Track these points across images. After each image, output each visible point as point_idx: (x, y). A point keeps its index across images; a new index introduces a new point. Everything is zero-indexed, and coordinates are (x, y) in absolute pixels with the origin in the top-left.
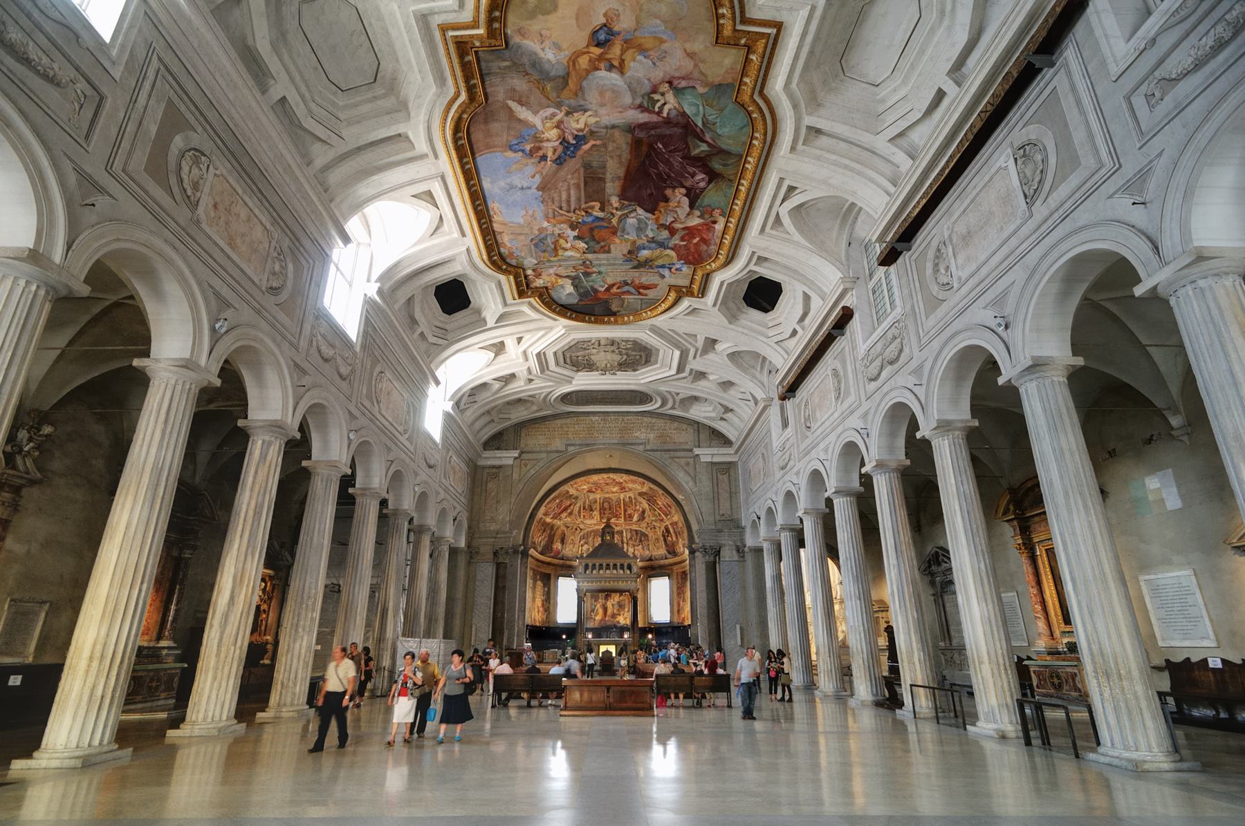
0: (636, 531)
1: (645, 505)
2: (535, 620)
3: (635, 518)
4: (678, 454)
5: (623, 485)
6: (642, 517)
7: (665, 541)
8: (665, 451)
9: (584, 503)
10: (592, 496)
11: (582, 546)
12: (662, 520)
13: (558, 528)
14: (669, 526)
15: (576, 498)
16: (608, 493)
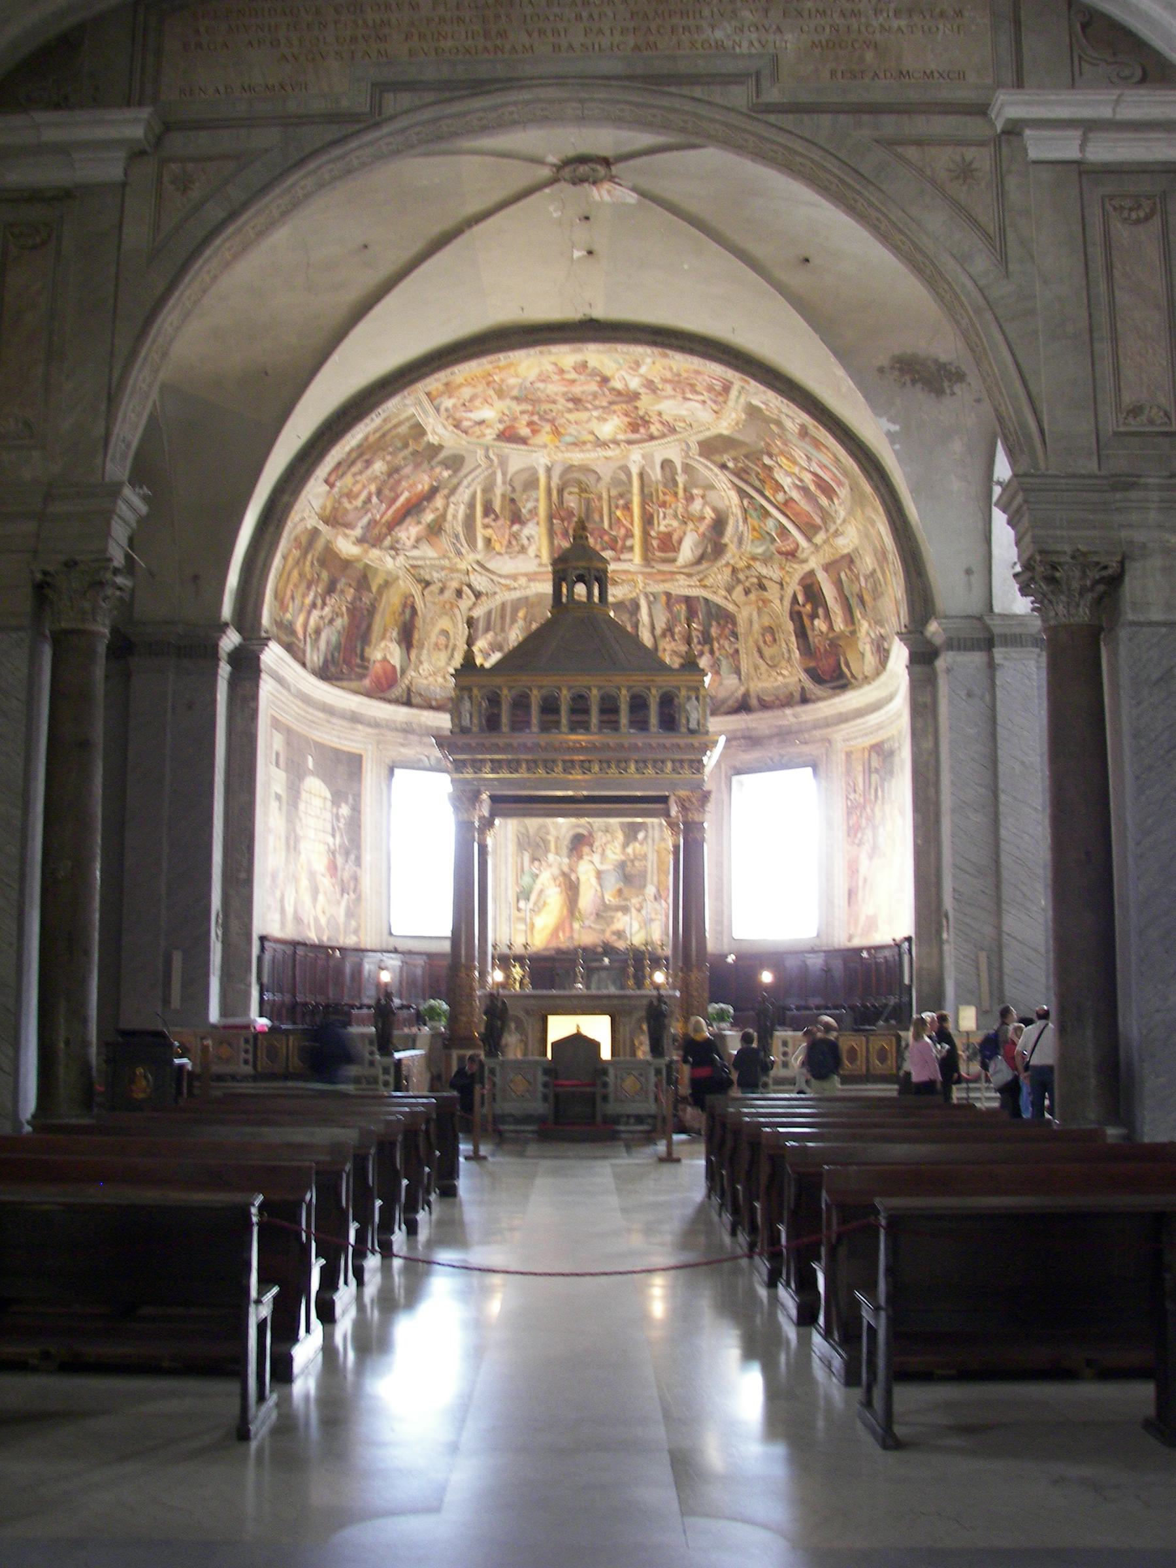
0: (688, 600)
1: (727, 496)
2: (298, 920)
3: (687, 552)
4: (920, 125)
5: (646, 404)
6: (713, 547)
7: (802, 634)
8: (858, 109)
9: (488, 489)
10: (518, 459)
11: (487, 656)
12: (792, 555)
13: (387, 584)
14: (822, 576)
15: (455, 463)
16: (578, 444)
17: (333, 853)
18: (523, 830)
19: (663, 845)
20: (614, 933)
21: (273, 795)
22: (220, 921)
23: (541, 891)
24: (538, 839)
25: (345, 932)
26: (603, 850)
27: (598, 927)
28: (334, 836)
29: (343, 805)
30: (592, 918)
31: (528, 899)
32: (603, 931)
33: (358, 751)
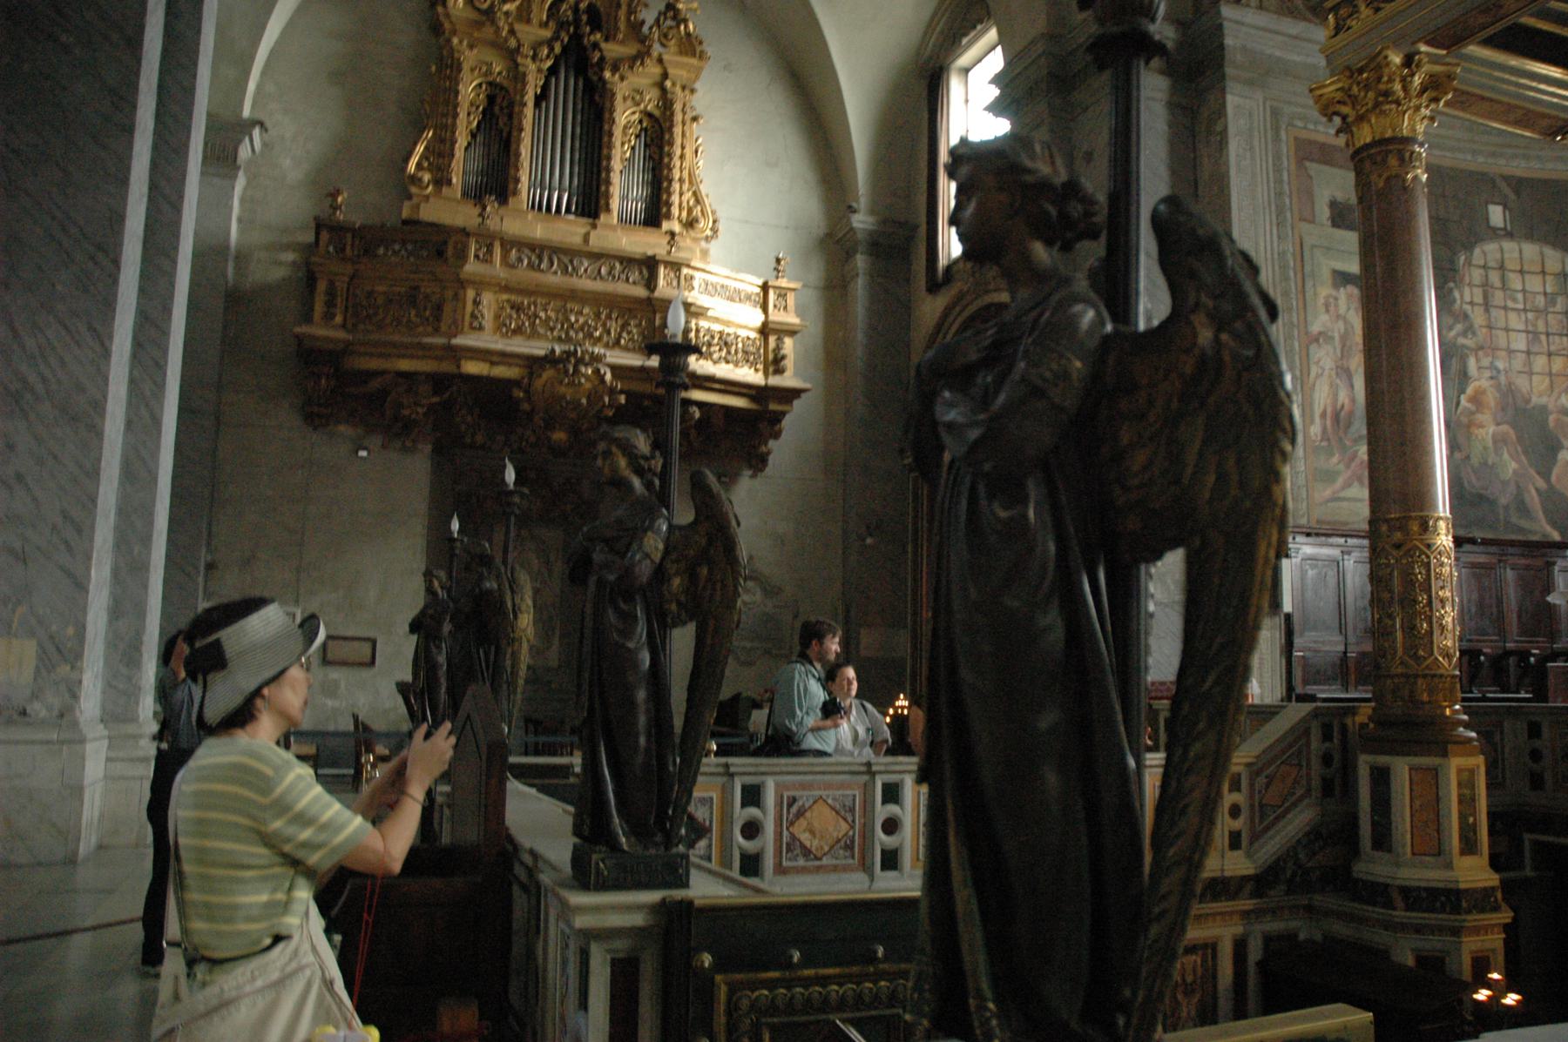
21: (1326, 274)
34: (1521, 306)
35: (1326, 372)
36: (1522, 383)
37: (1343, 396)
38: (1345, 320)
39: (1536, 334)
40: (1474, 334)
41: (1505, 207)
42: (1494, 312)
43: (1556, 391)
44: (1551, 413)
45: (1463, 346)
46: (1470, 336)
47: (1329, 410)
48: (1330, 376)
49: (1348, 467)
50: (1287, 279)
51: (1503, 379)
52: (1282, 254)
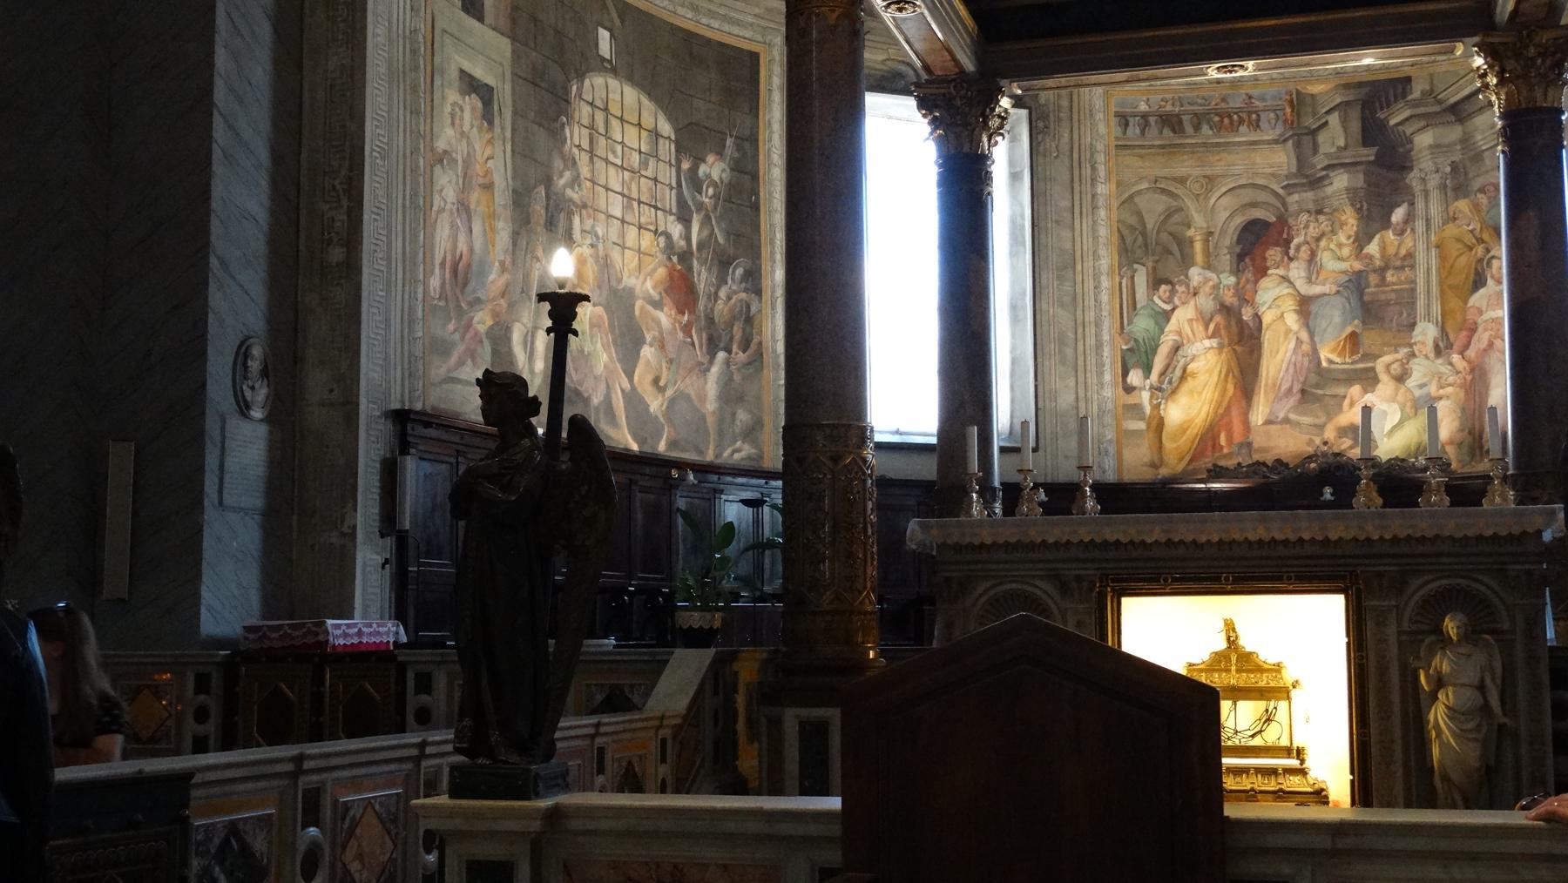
17: (685, 256)
18: (1132, 220)
19: (1451, 230)
20: (1344, 431)
21: (453, 74)
22: (255, 365)
23: (1177, 348)
24: (1164, 236)
25: (720, 432)
26: (1313, 254)
27: (1306, 420)
28: (684, 219)
29: (711, 158)
30: (1293, 400)
31: (1147, 369)
32: (1321, 427)
33: (746, 46)
34: (620, 164)
35: (448, 207)
36: (616, 255)
37: (462, 246)
38: (469, 144)
39: (630, 198)
40: (579, 186)
41: (612, 36)
42: (599, 164)
43: (642, 273)
44: (638, 298)
45: (571, 200)
46: (577, 188)
47: (449, 258)
48: (452, 213)
49: (462, 338)
50: (416, 68)
51: (600, 247)
52: (415, 31)
